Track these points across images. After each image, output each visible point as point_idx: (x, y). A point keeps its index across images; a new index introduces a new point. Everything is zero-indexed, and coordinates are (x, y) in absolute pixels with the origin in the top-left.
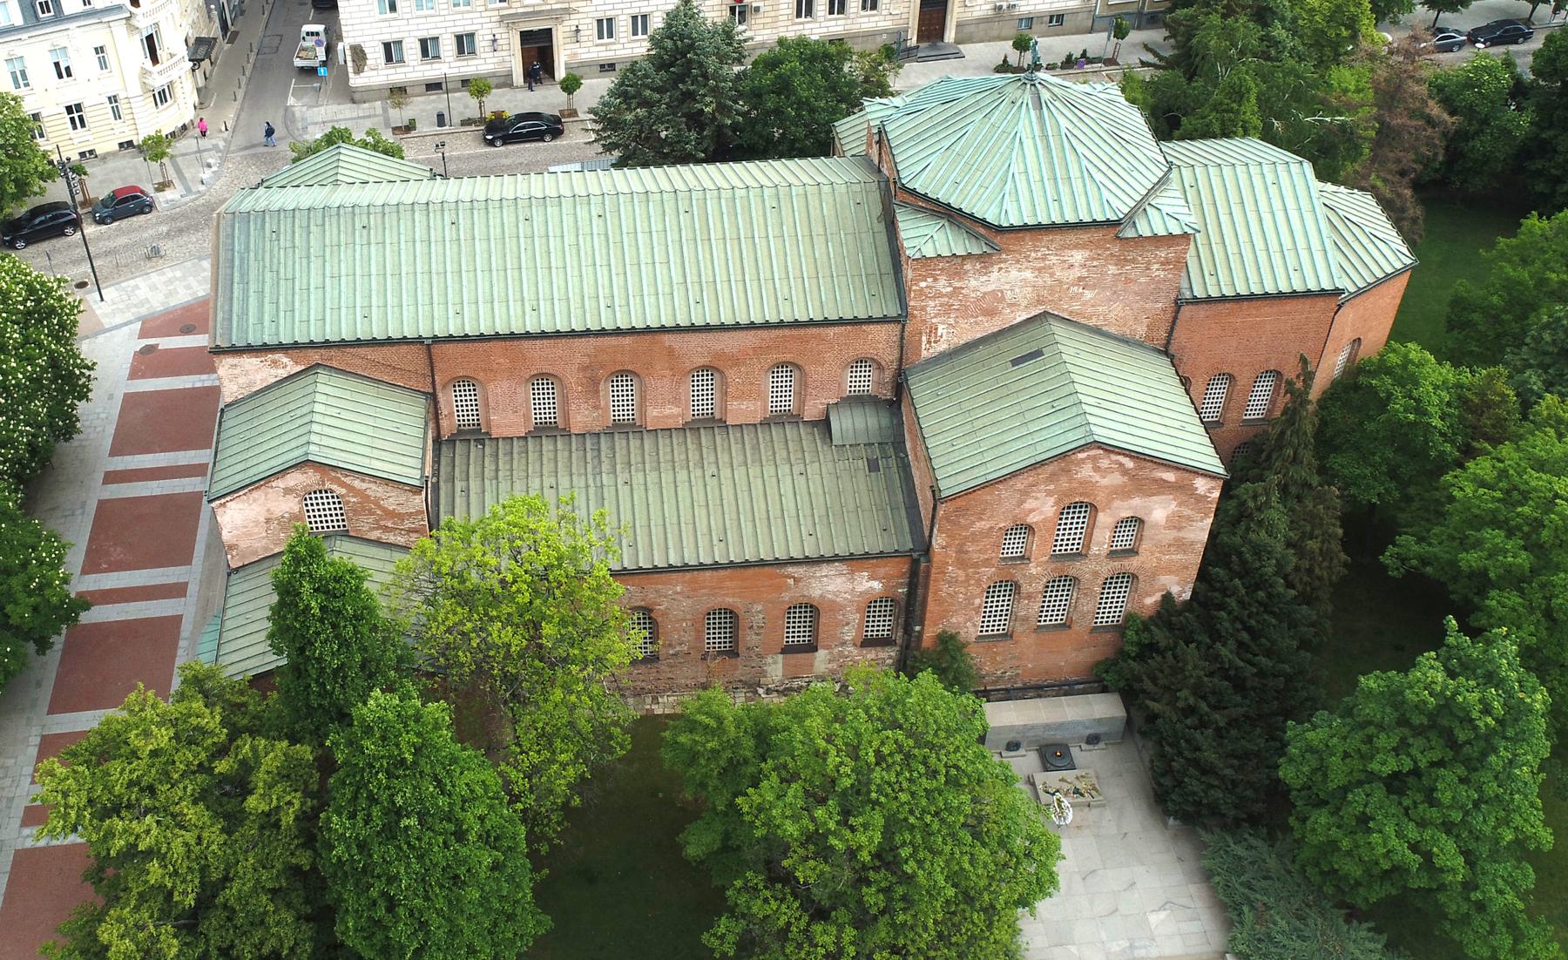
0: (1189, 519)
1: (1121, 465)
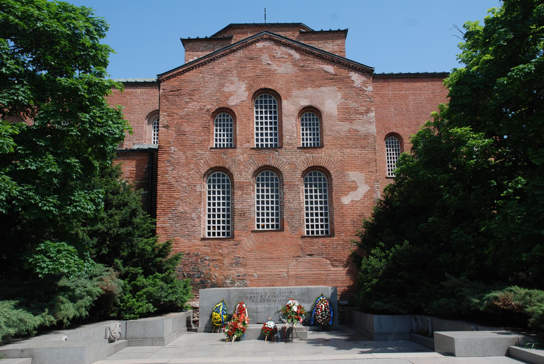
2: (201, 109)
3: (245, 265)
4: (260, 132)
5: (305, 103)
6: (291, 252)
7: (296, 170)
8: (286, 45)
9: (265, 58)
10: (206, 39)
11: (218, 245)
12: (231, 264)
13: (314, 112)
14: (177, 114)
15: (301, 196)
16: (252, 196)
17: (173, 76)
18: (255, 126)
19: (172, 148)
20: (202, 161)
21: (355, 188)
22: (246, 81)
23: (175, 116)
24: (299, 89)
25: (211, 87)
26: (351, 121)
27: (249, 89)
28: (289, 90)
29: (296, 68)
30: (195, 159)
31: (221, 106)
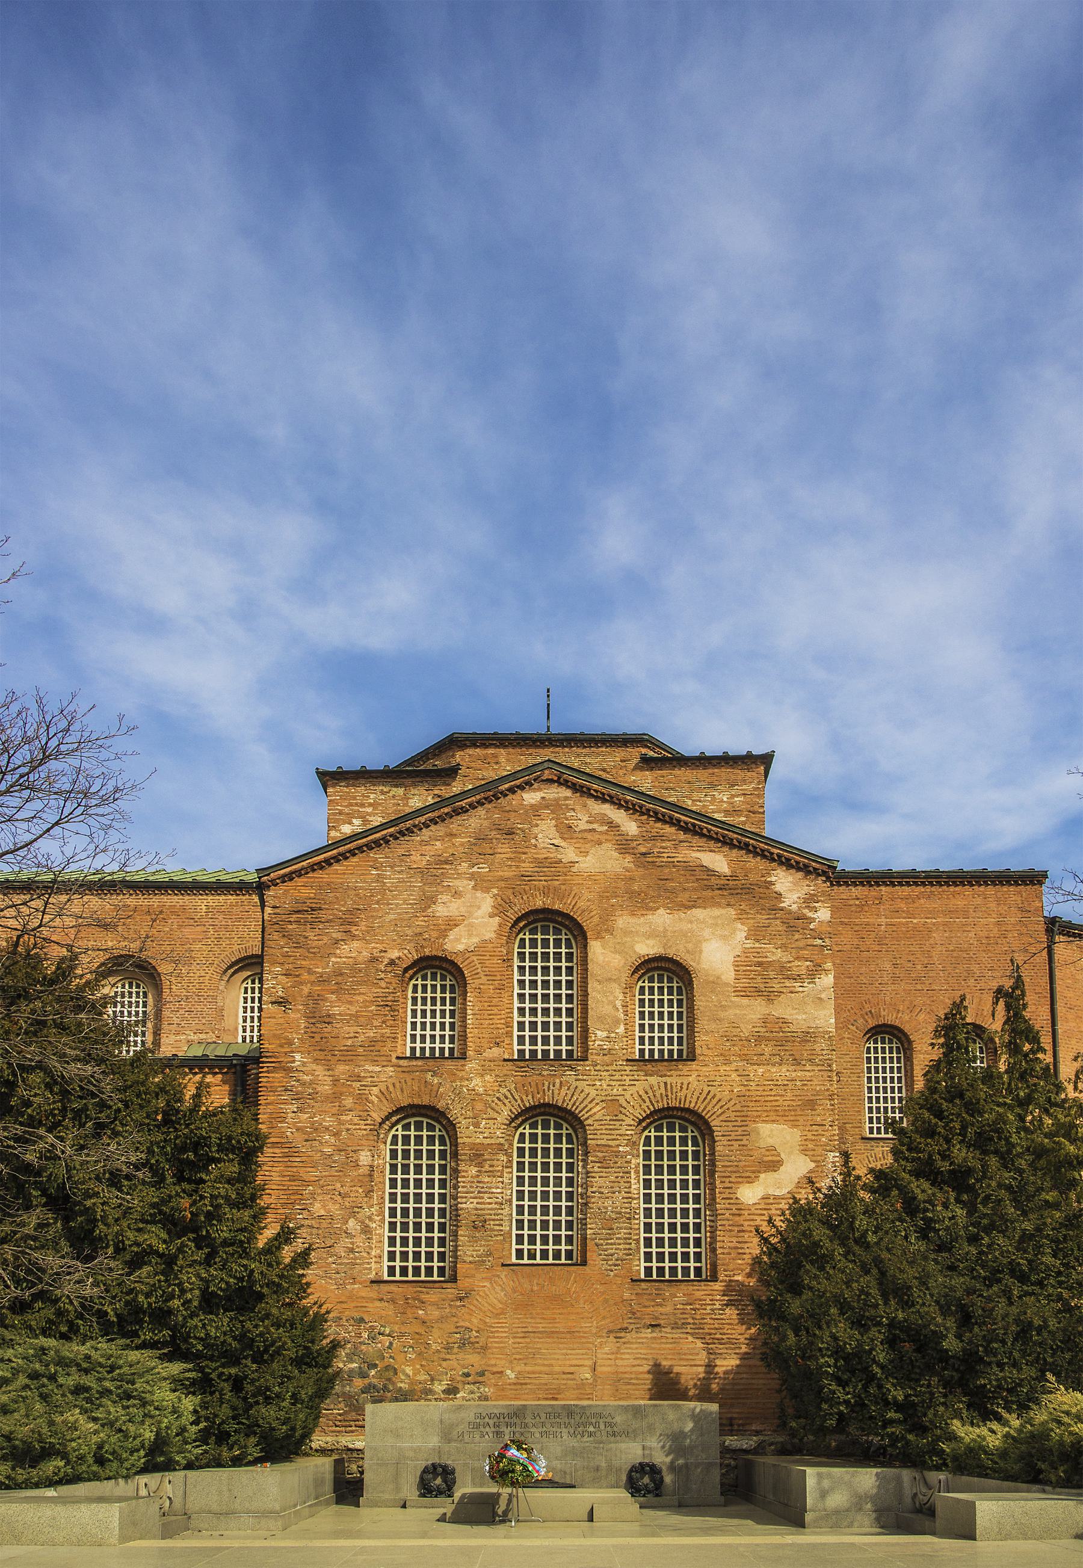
0: (783, 971)
1: (612, 826)
3: (485, 1348)
4: (527, 1019)
5: (647, 948)
6: (604, 1318)
7: (621, 1117)
8: (602, 798)
9: (545, 832)
11: (414, 1299)
12: (448, 1348)
13: (674, 972)
14: (310, 972)
15: (633, 1181)
16: (506, 1181)
17: (299, 873)
18: (516, 1004)
19: (298, 1056)
20: (375, 1090)
21: (774, 1165)
22: (495, 891)
23: (305, 976)
25: (402, 902)
26: (770, 996)
27: (499, 910)
28: (607, 917)
29: (629, 858)
30: (357, 1085)
31: (427, 952)
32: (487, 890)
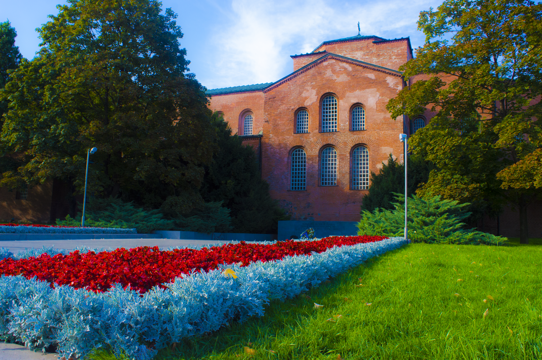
1: (345, 69)
2: (289, 109)
5: (354, 101)
9: (328, 73)
10: (307, 55)
24: (350, 92)
27: (317, 94)
31: (300, 106)
32: (315, 89)
